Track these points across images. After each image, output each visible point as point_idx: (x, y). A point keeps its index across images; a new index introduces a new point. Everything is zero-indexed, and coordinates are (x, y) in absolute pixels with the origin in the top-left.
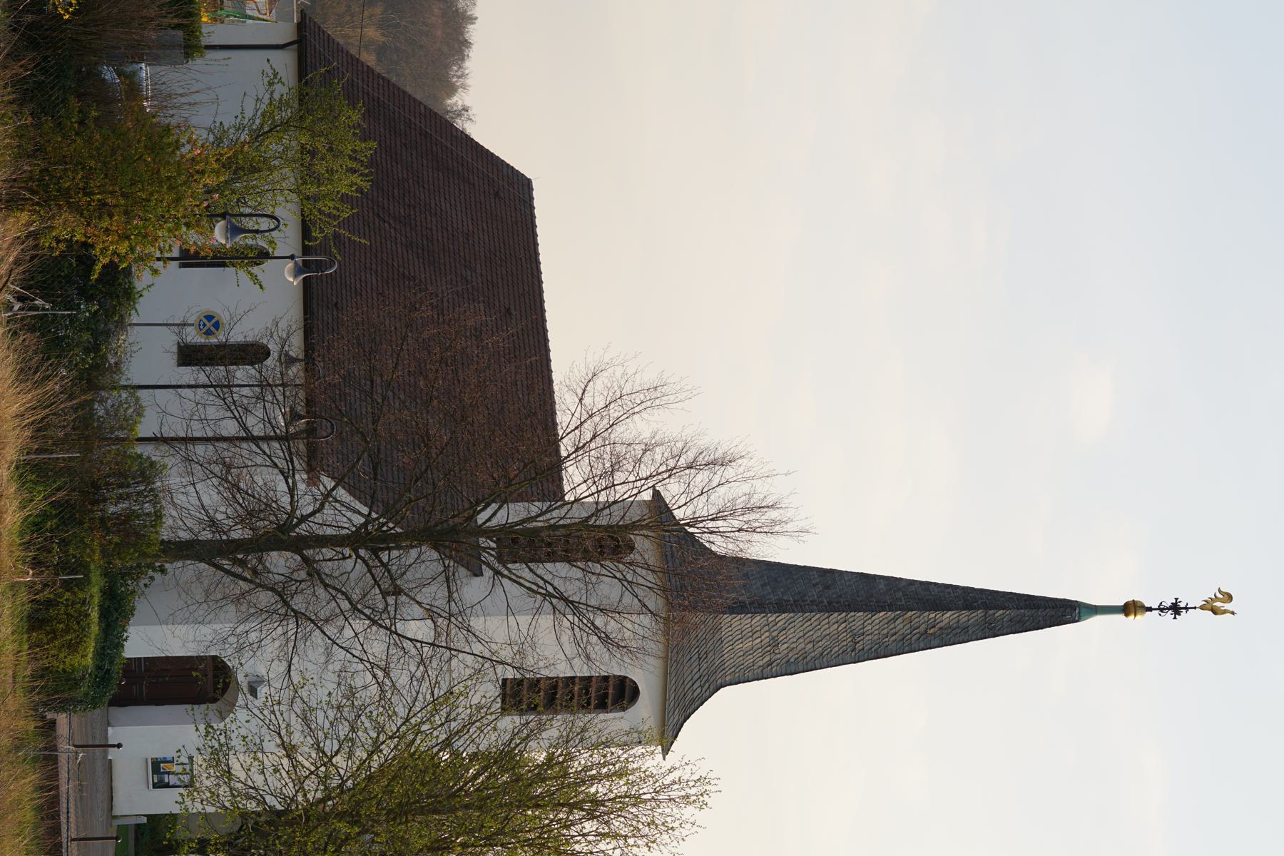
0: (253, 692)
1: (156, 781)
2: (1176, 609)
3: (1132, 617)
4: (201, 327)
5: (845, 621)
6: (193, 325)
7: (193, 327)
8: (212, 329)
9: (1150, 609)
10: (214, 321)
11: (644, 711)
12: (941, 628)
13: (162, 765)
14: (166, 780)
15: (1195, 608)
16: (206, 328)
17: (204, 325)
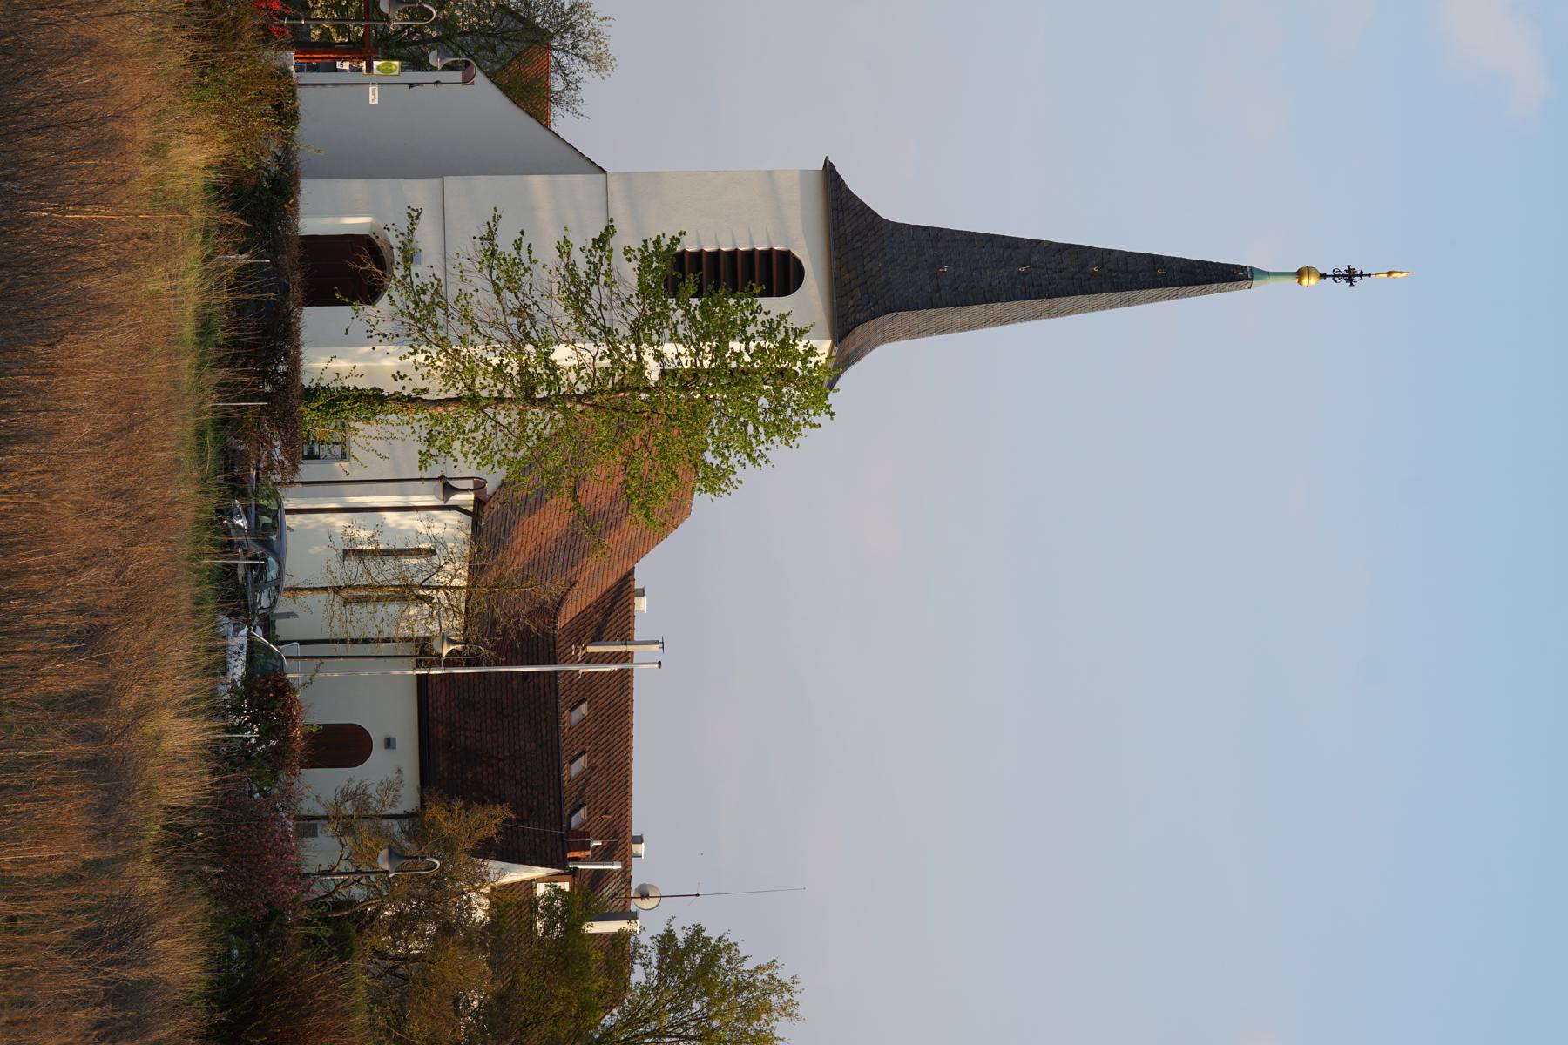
1: (305, 453)
2: (1350, 276)
3: (1305, 281)
5: (1010, 248)
9: (1324, 276)
12: (1110, 271)
14: (316, 450)
15: (1370, 275)
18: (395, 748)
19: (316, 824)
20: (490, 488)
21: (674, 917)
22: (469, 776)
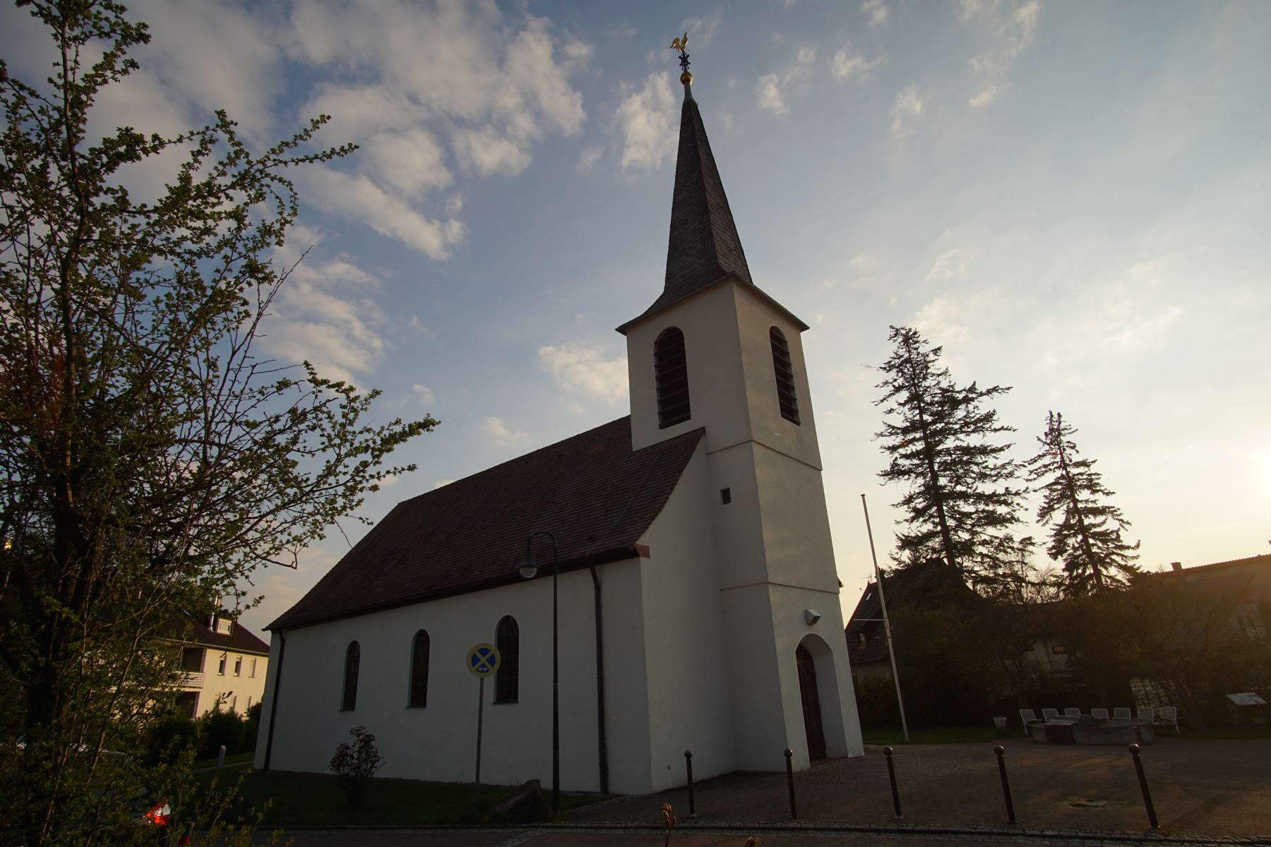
0: (816, 619)
4: (485, 669)
6: (482, 680)
7: (485, 680)
8: (488, 656)
10: (479, 655)
11: (786, 331)
16: (487, 664)
17: (483, 666)
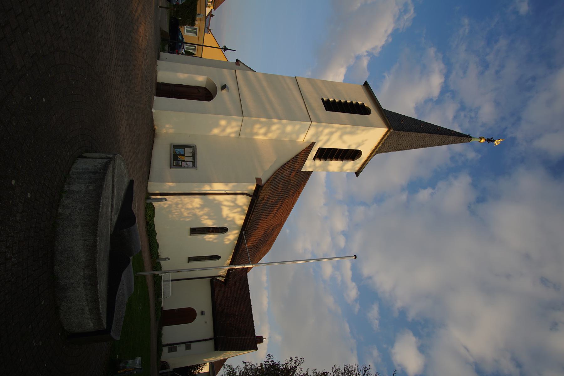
1: (175, 164)
13: (178, 156)
14: (180, 164)
18: (204, 315)
19: (176, 346)
20: (263, 181)
21: (308, 369)
22: (228, 322)
